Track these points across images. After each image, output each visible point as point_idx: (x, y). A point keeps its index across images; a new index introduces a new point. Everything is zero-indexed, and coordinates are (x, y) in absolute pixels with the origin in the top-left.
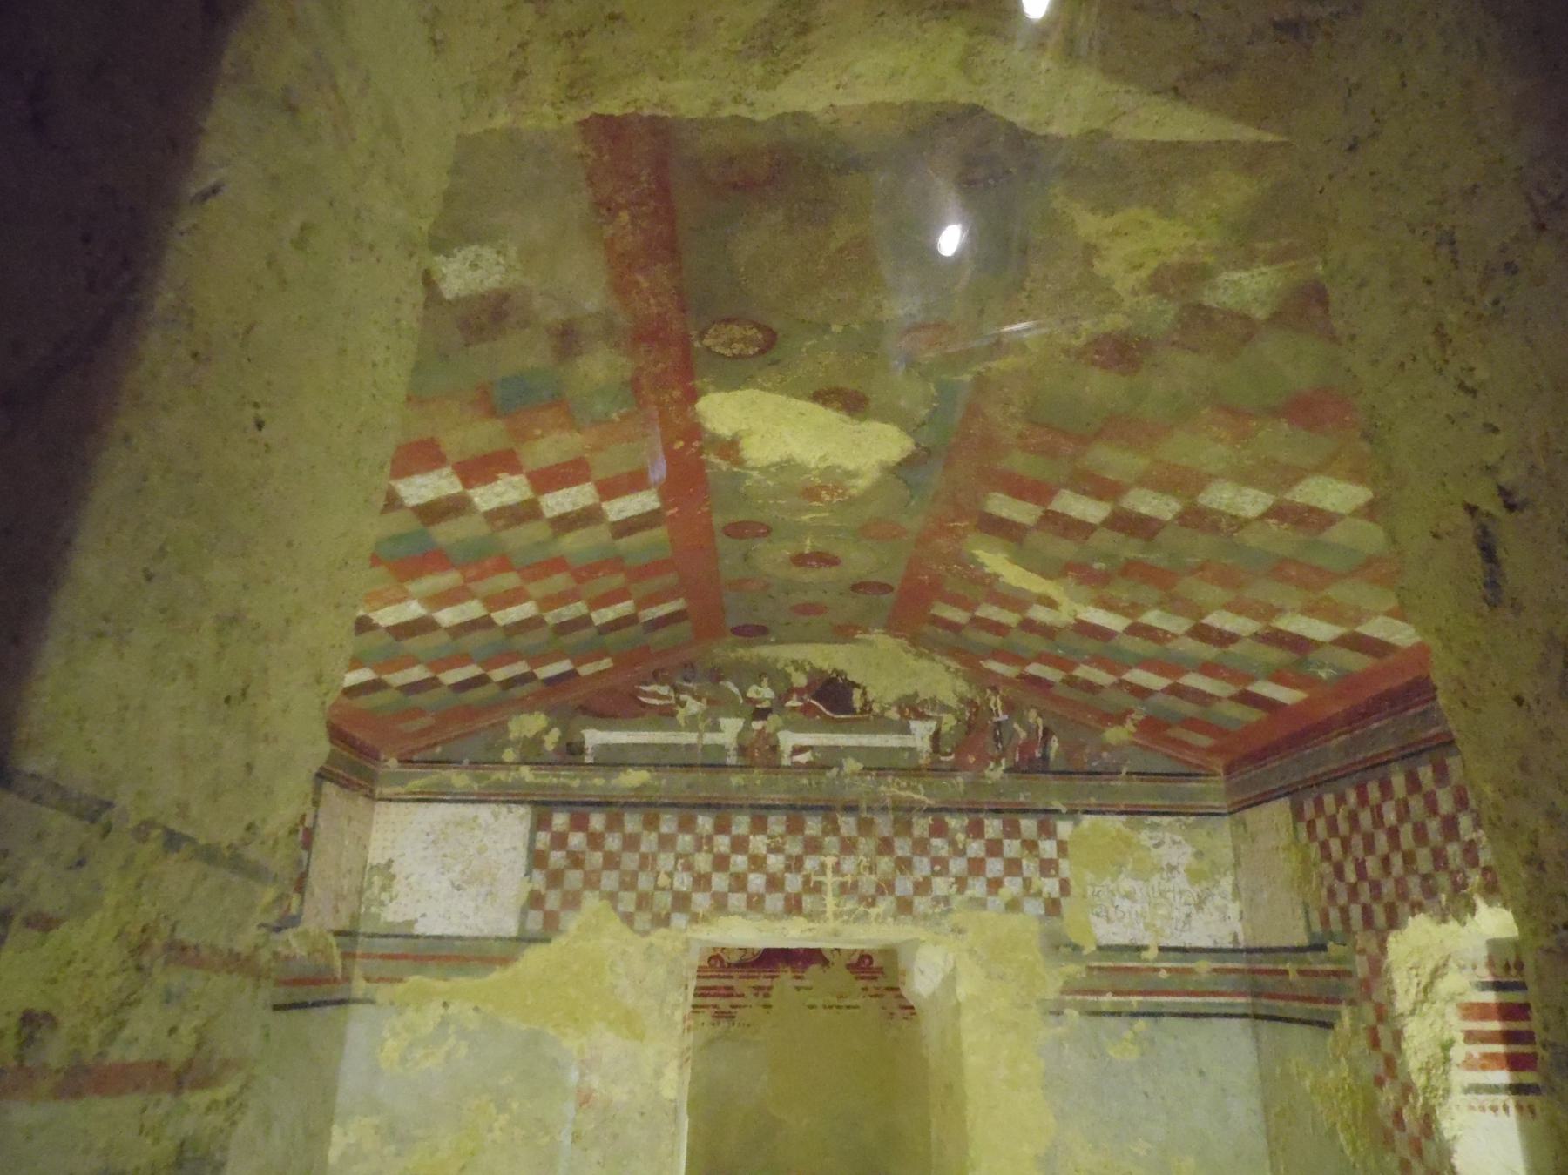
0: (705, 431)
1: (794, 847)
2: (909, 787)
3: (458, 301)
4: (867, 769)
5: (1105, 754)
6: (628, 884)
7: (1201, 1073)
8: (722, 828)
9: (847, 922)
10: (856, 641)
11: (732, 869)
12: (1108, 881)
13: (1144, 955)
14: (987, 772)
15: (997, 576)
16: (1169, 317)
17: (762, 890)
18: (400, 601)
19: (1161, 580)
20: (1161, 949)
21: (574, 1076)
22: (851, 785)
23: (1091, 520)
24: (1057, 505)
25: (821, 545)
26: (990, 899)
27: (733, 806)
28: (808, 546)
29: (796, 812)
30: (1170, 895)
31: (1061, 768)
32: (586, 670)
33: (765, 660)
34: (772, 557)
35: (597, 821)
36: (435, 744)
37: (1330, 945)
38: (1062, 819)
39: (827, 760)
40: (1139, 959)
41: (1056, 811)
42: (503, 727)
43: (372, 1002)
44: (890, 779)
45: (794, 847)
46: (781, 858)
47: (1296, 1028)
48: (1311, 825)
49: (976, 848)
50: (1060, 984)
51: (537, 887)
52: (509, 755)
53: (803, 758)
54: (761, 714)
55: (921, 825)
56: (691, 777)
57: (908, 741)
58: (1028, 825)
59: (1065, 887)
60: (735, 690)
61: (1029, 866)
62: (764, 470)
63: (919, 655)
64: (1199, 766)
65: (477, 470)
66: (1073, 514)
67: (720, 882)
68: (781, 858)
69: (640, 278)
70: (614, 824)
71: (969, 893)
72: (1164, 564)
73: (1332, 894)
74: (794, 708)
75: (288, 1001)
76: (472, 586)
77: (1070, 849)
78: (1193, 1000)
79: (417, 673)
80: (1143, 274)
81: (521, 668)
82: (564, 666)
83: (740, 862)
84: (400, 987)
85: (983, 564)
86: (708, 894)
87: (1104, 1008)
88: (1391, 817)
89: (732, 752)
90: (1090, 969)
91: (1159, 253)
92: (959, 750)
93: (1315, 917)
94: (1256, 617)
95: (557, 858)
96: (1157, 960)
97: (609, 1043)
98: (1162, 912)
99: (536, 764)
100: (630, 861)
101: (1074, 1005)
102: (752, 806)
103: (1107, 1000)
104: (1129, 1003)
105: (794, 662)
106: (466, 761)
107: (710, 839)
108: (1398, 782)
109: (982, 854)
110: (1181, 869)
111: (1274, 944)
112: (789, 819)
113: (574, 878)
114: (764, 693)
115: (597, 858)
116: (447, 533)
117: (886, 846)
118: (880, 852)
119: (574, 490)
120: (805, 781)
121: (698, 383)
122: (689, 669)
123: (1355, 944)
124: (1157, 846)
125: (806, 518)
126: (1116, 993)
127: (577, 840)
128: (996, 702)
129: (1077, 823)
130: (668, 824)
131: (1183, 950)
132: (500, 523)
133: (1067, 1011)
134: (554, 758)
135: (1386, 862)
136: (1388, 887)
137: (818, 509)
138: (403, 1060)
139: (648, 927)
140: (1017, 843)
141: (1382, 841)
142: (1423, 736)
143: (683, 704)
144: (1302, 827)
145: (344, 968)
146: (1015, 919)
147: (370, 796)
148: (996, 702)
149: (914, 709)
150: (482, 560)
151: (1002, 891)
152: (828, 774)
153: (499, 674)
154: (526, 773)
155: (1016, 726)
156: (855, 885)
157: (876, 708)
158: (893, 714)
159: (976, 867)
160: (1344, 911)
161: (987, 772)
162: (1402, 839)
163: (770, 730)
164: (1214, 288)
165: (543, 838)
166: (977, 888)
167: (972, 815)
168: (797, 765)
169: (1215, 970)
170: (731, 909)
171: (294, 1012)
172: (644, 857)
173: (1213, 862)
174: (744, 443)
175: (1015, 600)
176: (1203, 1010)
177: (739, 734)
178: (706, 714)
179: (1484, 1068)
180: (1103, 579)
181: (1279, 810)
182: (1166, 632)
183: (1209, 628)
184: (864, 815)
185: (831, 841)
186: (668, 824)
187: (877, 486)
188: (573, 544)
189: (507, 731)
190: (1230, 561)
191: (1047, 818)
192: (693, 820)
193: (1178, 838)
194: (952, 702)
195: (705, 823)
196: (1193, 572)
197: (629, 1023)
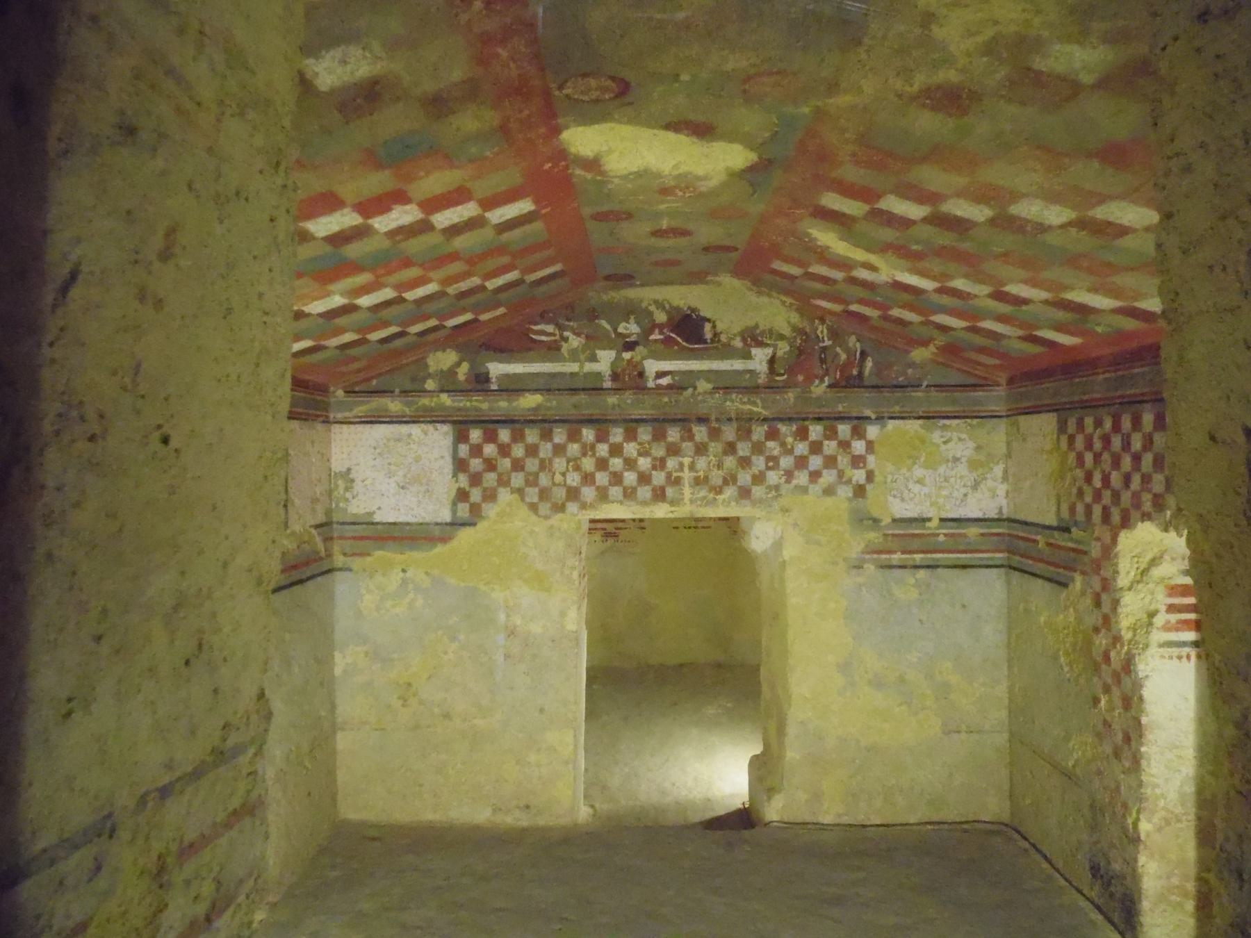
1: (659, 451)
2: (750, 402)
3: (333, 92)
4: (716, 389)
5: (910, 371)
6: (532, 481)
7: (964, 606)
8: (602, 438)
10: (707, 283)
11: (611, 469)
12: (904, 470)
13: (928, 524)
15: (828, 247)
17: (635, 484)
19: (971, 263)
20: (942, 520)
21: (502, 617)
24: (884, 204)
25: (674, 224)
26: (811, 486)
27: (610, 421)
28: (665, 224)
29: (660, 424)
31: (874, 383)
32: (484, 317)
34: (635, 233)
35: (504, 435)
37: (1074, 530)
38: (871, 424)
39: (682, 383)
40: (925, 528)
41: (868, 418)
42: (422, 363)
43: (351, 570)
44: (734, 396)
45: (659, 451)
46: (649, 460)
47: (1040, 581)
48: (1071, 439)
49: (801, 448)
50: (863, 545)
51: (462, 486)
52: (430, 385)
53: (665, 381)
54: (630, 346)
55: (759, 432)
56: (575, 399)
57: (750, 365)
58: (844, 429)
59: (870, 476)
60: (608, 327)
61: (843, 461)
63: (759, 293)
64: (985, 378)
65: (374, 206)
67: (602, 478)
68: (649, 460)
69: (500, 50)
70: (518, 437)
71: (795, 482)
73: (1080, 493)
74: (656, 341)
75: (288, 582)
76: (383, 280)
77: (876, 446)
78: (964, 556)
79: (348, 337)
80: (980, 39)
81: (433, 322)
84: (369, 559)
86: (593, 488)
87: (895, 563)
88: (1137, 445)
89: (607, 378)
90: (885, 535)
92: (791, 371)
93: (1065, 508)
94: (1048, 290)
95: (476, 464)
96: (938, 528)
97: (526, 595)
98: (944, 493)
100: (532, 465)
101: (874, 561)
102: (625, 421)
103: (897, 557)
104: (914, 560)
105: (656, 302)
106: (397, 390)
107: (593, 447)
110: (964, 460)
111: (1030, 519)
112: (654, 429)
113: (490, 479)
114: (631, 328)
115: (506, 463)
116: (353, 251)
117: (731, 448)
118: (725, 453)
119: (459, 208)
120: (666, 399)
124: (945, 443)
125: (663, 207)
126: (903, 552)
127: (490, 450)
128: (822, 331)
129: (884, 426)
130: (560, 436)
133: (866, 566)
134: (470, 387)
135: (1127, 479)
136: (1126, 497)
138: (378, 609)
139: (548, 512)
140: (834, 444)
141: (1127, 462)
143: (566, 340)
144: (1064, 439)
146: (829, 501)
147: (327, 421)
148: (822, 331)
150: (386, 264)
151: (821, 480)
153: (414, 329)
154: (445, 399)
155: (838, 349)
156: (706, 478)
157: (723, 338)
158: (738, 343)
159: (801, 462)
160: (1088, 510)
163: (638, 358)
165: (464, 450)
166: (802, 478)
168: (659, 387)
169: (982, 535)
170: (611, 498)
171: (295, 588)
172: (542, 462)
174: (603, 161)
177: (613, 364)
178: (585, 348)
179: (1177, 630)
180: (918, 256)
182: (969, 294)
183: (1007, 294)
184: (714, 425)
185: (688, 446)
186: (560, 436)
187: (724, 186)
188: (461, 243)
189: (427, 366)
191: (859, 424)
192: (579, 432)
193: (964, 436)
194: (787, 331)
195: (588, 434)
197: (540, 581)
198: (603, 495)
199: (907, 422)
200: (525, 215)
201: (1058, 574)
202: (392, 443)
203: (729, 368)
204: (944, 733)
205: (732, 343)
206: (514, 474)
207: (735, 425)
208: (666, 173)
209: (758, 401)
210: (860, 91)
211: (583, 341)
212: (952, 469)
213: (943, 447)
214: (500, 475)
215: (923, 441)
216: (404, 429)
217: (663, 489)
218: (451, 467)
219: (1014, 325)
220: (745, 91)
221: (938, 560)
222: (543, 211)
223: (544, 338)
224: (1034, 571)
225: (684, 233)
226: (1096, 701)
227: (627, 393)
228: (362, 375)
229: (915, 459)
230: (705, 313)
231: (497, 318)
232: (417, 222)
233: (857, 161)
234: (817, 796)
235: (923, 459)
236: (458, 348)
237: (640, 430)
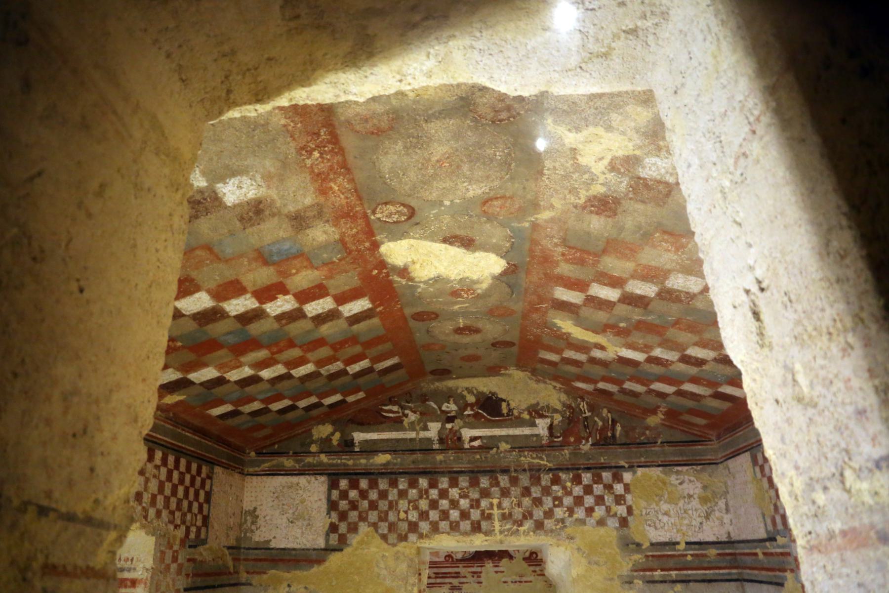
0: (388, 264)
1: (475, 495)
2: (537, 457)
6: (383, 518)
8: (433, 485)
9: (507, 535)
11: (441, 508)
12: (654, 505)
13: (678, 547)
15: (569, 334)
17: (458, 519)
18: (238, 367)
20: (687, 543)
22: (505, 457)
23: (612, 300)
25: (468, 323)
26: (588, 519)
27: (439, 472)
28: (461, 323)
29: (474, 475)
30: (690, 512)
31: (624, 440)
32: (351, 399)
33: (450, 389)
34: (443, 330)
36: (274, 444)
39: (489, 444)
40: (675, 550)
41: (623, 467)
42: (309, 432)
44: (526, 453)
46: (467, 501)
49: (578, 490)
50: (631, 565)
52: (314, 448)
53: (476, 443)
54: (451, 419)
55: (546, 479)
57: (535, 431)
58: (607, 476)
59: (630, 510)
60: (435, 406)
61: (609, 499)
62: (425, 282)
63: (538, 381)
66: (602, 296)
67: (434, 515)
68: (467, 501)
70: (373, 485)
71: (575, 516)
72: (657, 322)
74: (469, 415)
76: (276, 356)
77: (632, 488)
78: (707, 572)
79: (256, 406)
81: (313, 400)
82: (337, 398)
83: (444, 504)
85: (560, 327)
87: (657, 579)
90: (647, 556)
92: (566, 434)
95: (343, 505)
98: (686, 522)
99: (329, 452)
100: (383, 505)
102: (450, 472)
103: (658, 574)
104: (670, 575)
106: (291, 453)
107: (427, 492)
109: (581, 494)
110: (695, 496)
112: (470, 479)
113: (353, 515)
114: (451, 407)
117: (526, 492)
118: (523, 495)
119: (321, 301)
120: (478, 457)
121: (378, 238)
122: (409, 396)
124: (681, 484)
125: (456, 307)
126: (662, 570)
127: (353, 494)
128: (583, 406)
129: (635, 473)
130: (403, 484)
132: (284, 322)
133: (636, 581)
134: (340, 449)
137: (463, 303)
140: (601, 486)
143: (406, 416)
145: (234, 567)
146: (602, 530)
147: (242, 473)
148: (583, 406)
149: (537, 412)
150: (278, 344)
151: (594, 514)
153: (302, 404)
154: (324, 458)
155: (596, 419)
157: (516, 413)
158: (526, 416)
159: (579, 501)
163: (456, 428)
165: (335, 494)
166: (580, 513)
167: (575, 472)
168: (472, 448)
170: (441, 530)
172: (391, 503)
173: (714, 492)
174: (411, 268)
175: (583, 347)
177: (439, 432)
178: (419, 421)
182: (667, 360)
183: (690, 357)
184: (513, 474)
185: (495, 490)
187: (491, 288)
188: (326, 330)
192: (416, 481)
193: (692, 478)
194: (559, 406)
195: (423, 482)
198: (435, 528)
200: (365, 311)
201: (775, 576)
202: (285, 490)
203: (521, 433)
205: (522, 416)
206: (370, 512)
211: (419, 417)
212: (689, 503)
213: (680, 487)
214: (360, 513)
215: (664, 483)
216: (294, 479)
217: (479, 523)
218: (326, 506)
221: (689, 575)
222: (378, 310)
223: (391, 415)
224: (760, 579)
225: (477, 331)
227: (450, 452)
228: (268, 442)
229: (661, 497)
231: (358, 402)
232: (294, 310)
235: (666, 497)
236: (333, 423)
237: (461, 479)
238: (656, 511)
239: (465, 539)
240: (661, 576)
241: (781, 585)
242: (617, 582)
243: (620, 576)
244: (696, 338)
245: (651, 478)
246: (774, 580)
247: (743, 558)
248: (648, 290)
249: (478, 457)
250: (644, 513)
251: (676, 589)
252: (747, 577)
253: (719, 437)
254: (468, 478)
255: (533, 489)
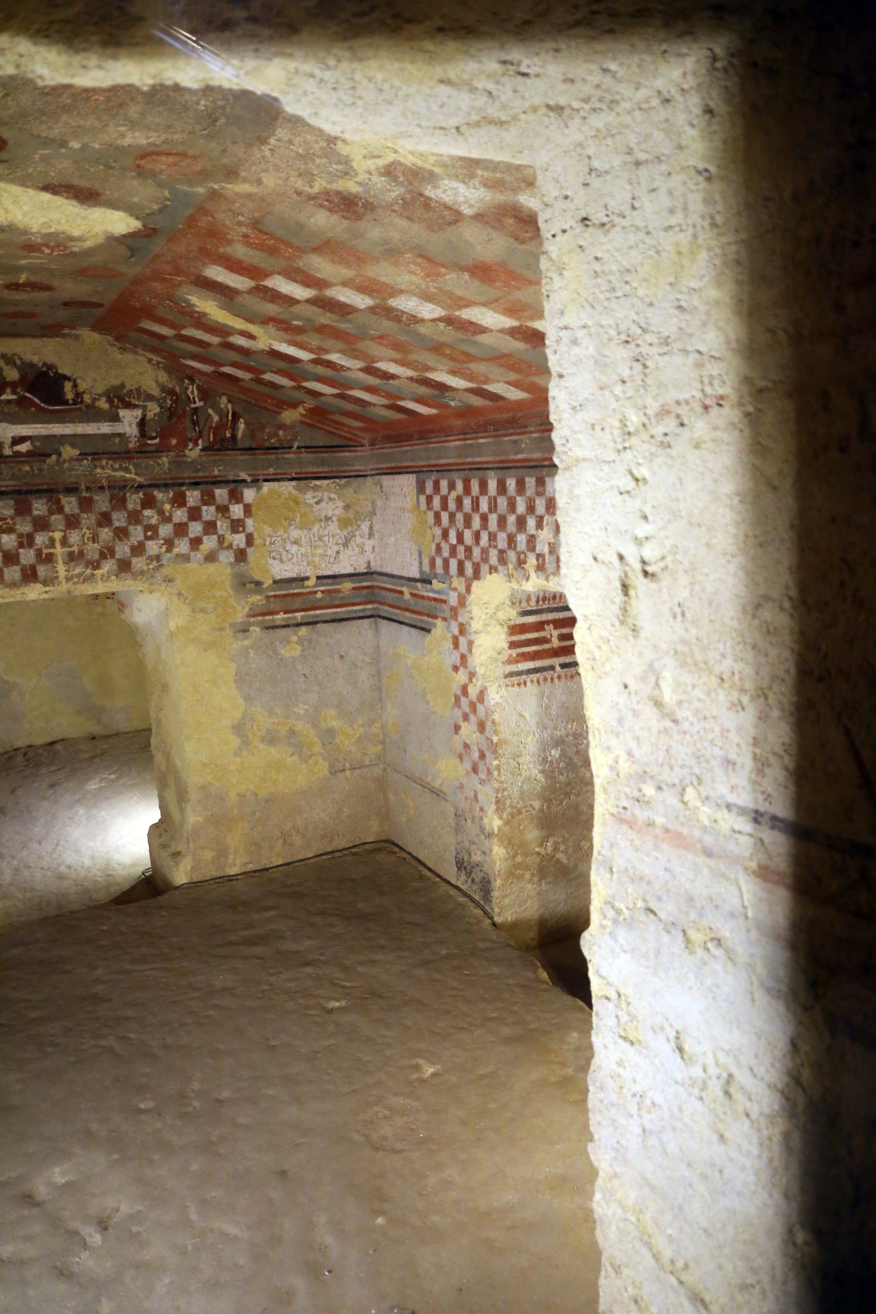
2: (121, 468)
5: (281, 433)
7: (342, 657)
9: (77, 583)
10: (64, 336)
13: (306, 583)
14: (187, 452)
16: (393, 195)
19: (349, 342)
20: (318, 578)
24: (270, 283)
25: (33, 279)
28: (23, 278)
30: (326, 539)
31: (247, 445)
37: (434, 581)
38: (248, 487)
39: (44, 450)
40: (303, 587)
41: (244, 481)
44: (104, 462)
46: (14, 537)
47: (405, 628)
48: (429, 499)
49: (180, 515)
50: (247, 609)
53: (23, 448)
57: (118, 428)
58: (221, 494)
61: (222, 526)
63: (123, 350)
68: (14, 537)
71: (176, 550)
72: (353, 331)
73: (439, 549)
74: (9, 402)
77: (254, 509)
78: (339, 610)
85: (194, 305)
87: (278, 623)
88: (484, 506)
90: (268, 597)
91: (396, 152)
92: (164, 435)
93: (426, 562)
94: (415, 369)
98: (320, 551)
104: (295, 618)
108: (492, 485)
109: (185, 520)
110: (334, 519)
111: (396, 572)
117: (105, 519)
118: (100, 525)
120: (27, 468)
123: (451, 584)
124: (317, 503)
125: (23, 262)
126: (286, 612)
128: (193, 391)
129: (259, 489)
131: (334, 577)
133: (251, 628)
135: (477, 536)
136: (476, 552)
140: (212, 509)
141: (476, 522)
142: (512, 457)
144: (423, 499)
146: (211, 568)
148: (193, 391)
149: (121, 399)
152: (48, 461)
155: (210, 411)
156: (81, 553)
157: (87, 399)
158: (103, 404)
159: (181, 530)
160: (446, 562)
161: (187, 452)
162: (490, 523)
164: (435, 187)
166: (182, 546)
167: (177, 489)
168: (17, 454)
169: (354, 589)
173: (357, 512)
176: (344, 616)
179: (517, 662)
180: (299, 330)
181: (408, 482)
182: (342, 366)
185: (56, 518)
190: (403, 338)
193: (333, 496)
194: (156, 392)
196: (372, 339)
199: (281, 483)
201: (421, 620)
203: (97, 432)
204: (331, 773)
205: (97, 404)
207: (107, 493)
208: (34, 230)
209: (131, 467)
210: (259, 182)
215: (297, 503)
217: (33, 568)
219: (380, 395)
220: (138, 166)
221: (317, 616)
224: (402, 619)
226: (457, 728)
230: (64, 370)
233: (248, 244)
234: (222, 853)
235: (298, 520)
238: (284, 540)
239: (12, 593)
240: (283, 619)
241: (428, 631)
242: (228, 632)
243: (231, 625)
244: (398, 356)
245: (280, 496)
246: (419, 624)
247: (383, 593)
248: (362, 301)
249: (27, 468)
250: (268, 543)
251: (300, 633)
252: (382, 614)
253: (373, 443)
254: (12, 502)
255: (115, 516)
